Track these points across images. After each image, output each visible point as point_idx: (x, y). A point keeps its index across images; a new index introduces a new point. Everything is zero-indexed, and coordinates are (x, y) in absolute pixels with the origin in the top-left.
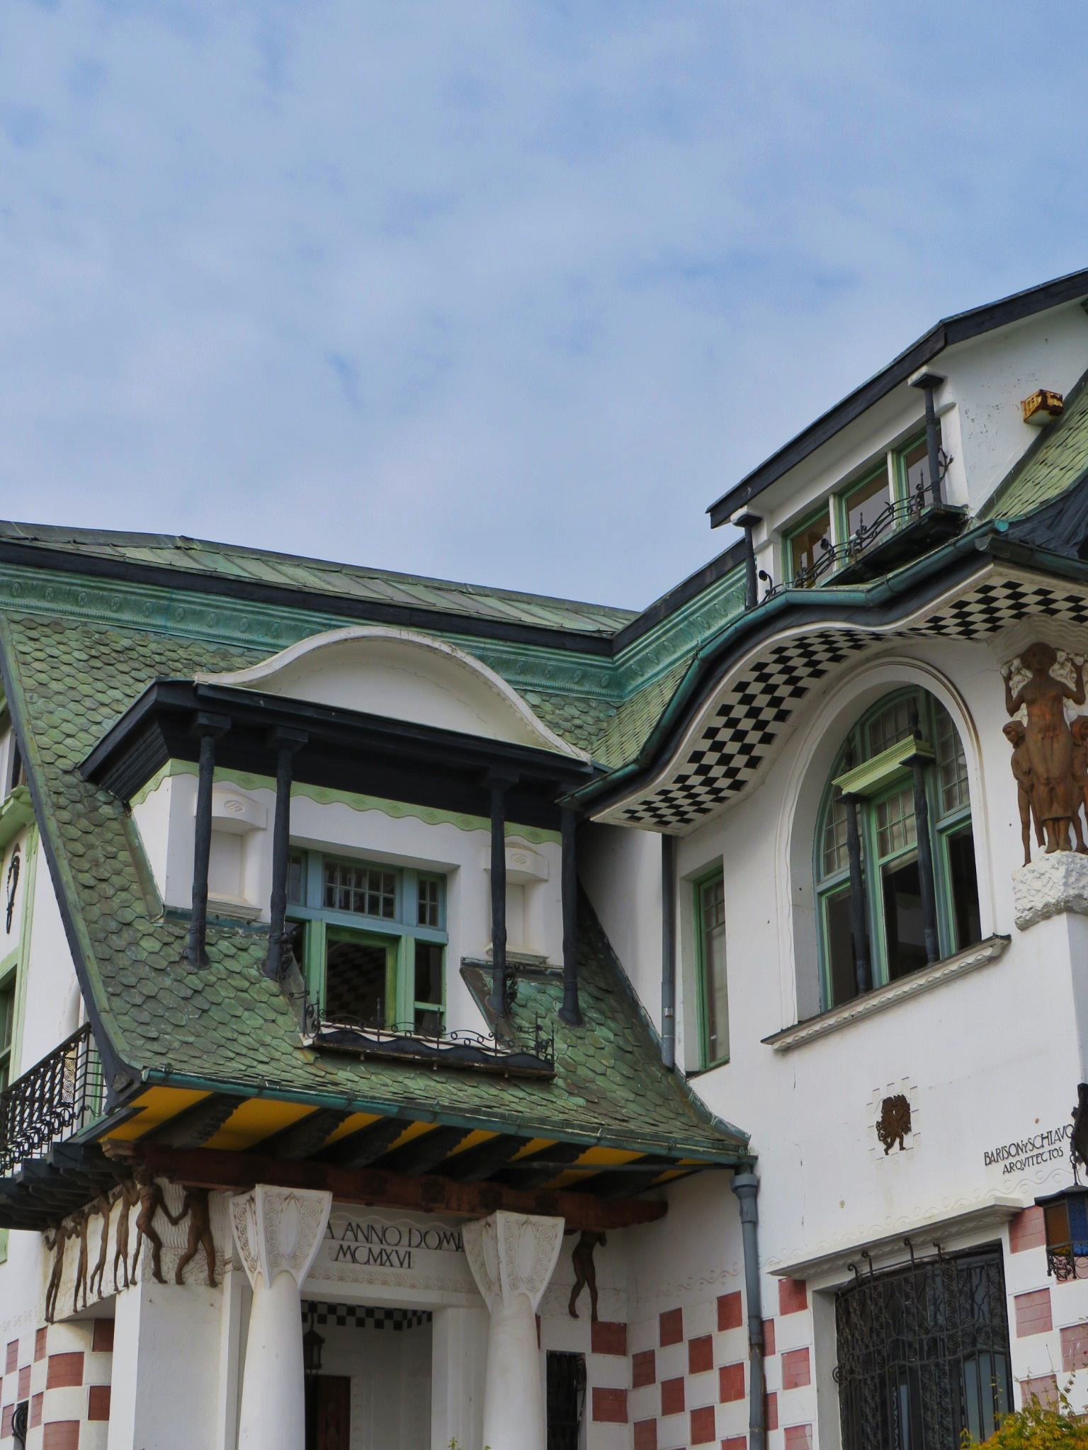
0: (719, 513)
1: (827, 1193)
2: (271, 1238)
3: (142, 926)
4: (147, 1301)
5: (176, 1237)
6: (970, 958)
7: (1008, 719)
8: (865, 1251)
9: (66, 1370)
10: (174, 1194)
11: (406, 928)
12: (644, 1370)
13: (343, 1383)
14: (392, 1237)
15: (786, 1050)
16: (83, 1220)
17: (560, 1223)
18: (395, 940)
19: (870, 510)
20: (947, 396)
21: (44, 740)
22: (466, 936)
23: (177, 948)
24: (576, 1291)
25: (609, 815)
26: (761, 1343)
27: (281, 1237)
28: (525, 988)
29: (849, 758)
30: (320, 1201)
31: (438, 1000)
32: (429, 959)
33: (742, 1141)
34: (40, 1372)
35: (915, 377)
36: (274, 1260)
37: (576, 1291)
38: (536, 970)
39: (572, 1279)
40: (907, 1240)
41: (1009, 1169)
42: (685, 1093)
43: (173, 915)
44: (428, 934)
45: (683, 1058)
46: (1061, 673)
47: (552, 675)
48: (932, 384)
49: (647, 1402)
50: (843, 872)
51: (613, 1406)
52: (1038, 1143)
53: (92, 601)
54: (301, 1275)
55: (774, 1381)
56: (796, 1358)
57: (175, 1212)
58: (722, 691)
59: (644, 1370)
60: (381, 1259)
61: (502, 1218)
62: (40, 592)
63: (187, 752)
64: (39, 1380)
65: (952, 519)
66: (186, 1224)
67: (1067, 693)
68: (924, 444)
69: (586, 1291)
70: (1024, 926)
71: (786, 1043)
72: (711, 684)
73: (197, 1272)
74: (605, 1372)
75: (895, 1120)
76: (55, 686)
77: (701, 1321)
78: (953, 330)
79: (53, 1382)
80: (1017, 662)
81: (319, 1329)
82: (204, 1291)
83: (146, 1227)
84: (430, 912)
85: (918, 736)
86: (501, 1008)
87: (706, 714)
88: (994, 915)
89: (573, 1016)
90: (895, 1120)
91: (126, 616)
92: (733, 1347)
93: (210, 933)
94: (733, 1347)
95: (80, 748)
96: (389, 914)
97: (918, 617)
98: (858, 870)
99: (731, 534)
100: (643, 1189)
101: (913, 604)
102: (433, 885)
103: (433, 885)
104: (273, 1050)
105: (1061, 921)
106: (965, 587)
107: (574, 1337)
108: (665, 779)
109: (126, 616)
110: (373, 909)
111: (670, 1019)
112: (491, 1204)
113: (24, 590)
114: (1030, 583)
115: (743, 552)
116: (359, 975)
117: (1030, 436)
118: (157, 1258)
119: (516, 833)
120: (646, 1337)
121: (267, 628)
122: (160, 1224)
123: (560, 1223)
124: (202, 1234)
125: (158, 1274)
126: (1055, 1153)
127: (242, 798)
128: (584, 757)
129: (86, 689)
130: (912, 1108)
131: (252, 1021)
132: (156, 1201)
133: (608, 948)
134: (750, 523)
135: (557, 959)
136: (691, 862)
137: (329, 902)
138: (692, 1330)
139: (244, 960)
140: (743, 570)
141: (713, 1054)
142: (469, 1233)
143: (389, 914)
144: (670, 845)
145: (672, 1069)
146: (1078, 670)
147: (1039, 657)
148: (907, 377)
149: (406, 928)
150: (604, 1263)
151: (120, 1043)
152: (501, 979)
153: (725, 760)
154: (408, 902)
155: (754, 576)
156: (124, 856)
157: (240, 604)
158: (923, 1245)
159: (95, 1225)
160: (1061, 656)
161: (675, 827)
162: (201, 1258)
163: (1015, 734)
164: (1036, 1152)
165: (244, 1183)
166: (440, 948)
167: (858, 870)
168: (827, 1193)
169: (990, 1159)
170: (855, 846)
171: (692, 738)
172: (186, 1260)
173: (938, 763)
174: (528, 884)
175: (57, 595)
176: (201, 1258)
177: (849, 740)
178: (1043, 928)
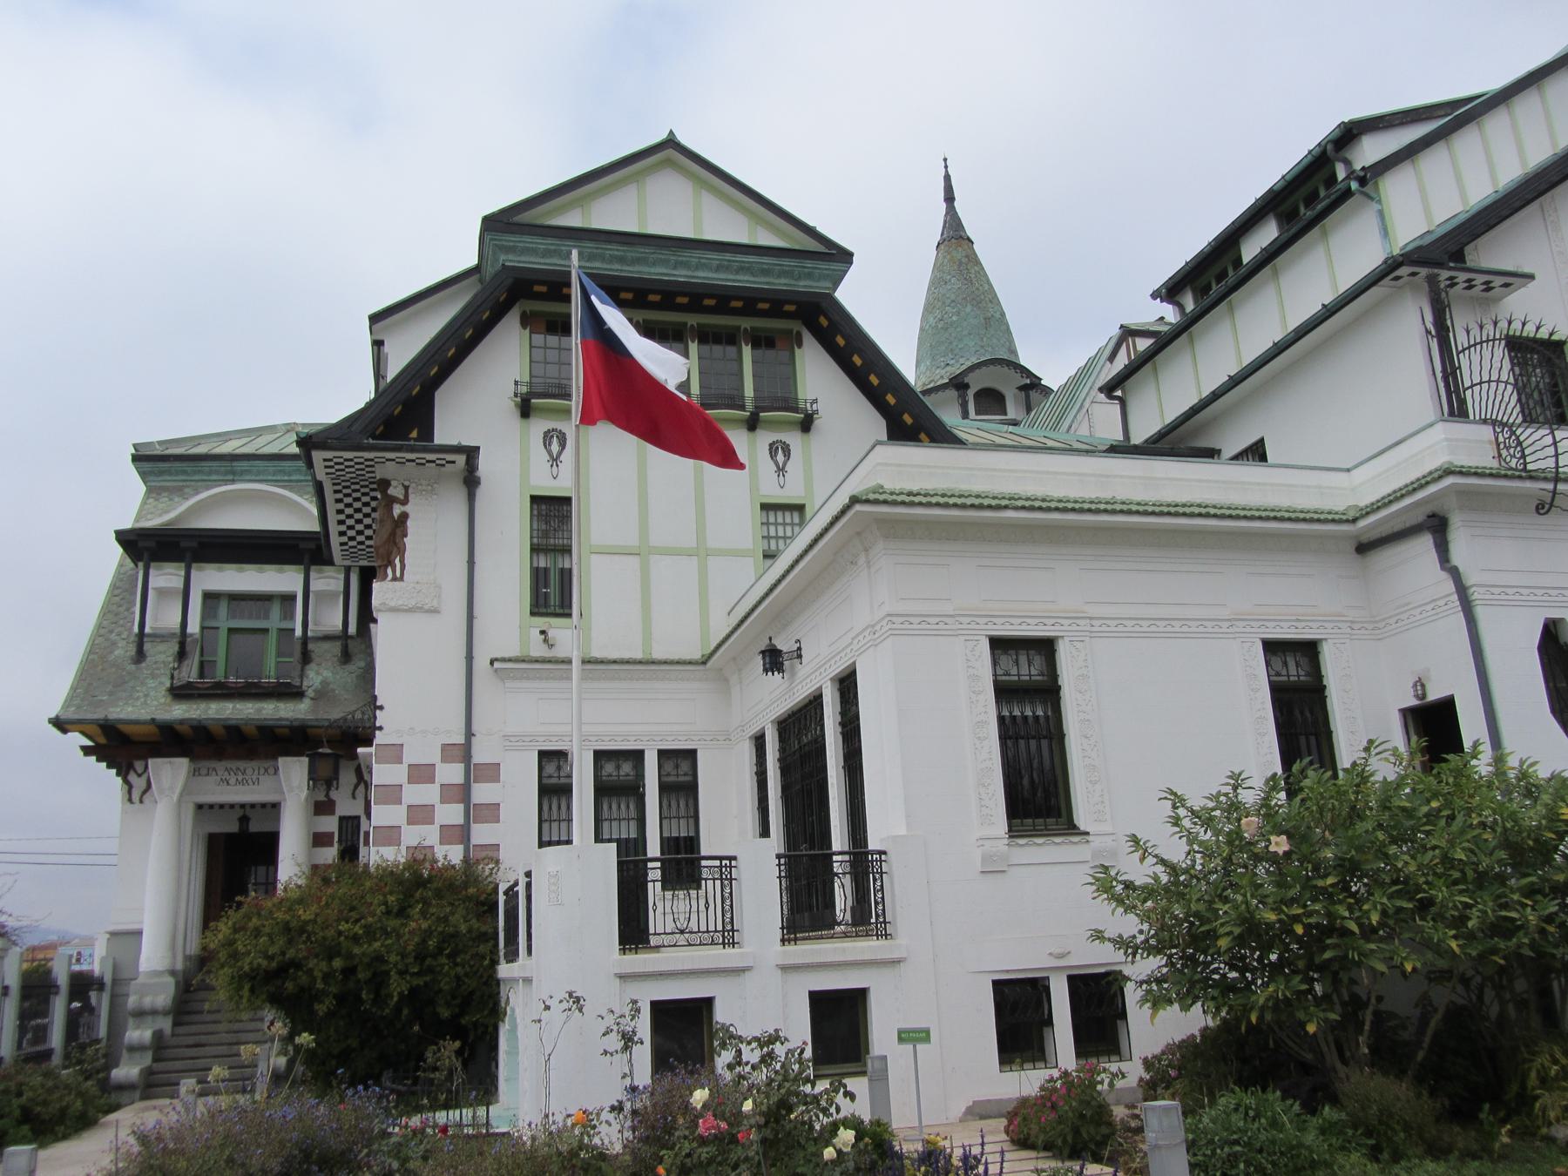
11: (274, 621)
14: (249, 771)
18: (267, 630)
24: (356, 787)
30: (183, 764)
37: (356, 787)
39: (354, 780)
44: (289, 626)
46: (395, 491)
53: (195, 473)
60: (243, 782)
61: (281, 760)
67: (394, 500)
69: (361, 788)
81: (249, 812)
84: (289, 614)
96: (267, 617)
102: (289, 599)
110: (258, 618)
118: (130, 792)
121: (283, 472)
125: (130, 800)
131: (151, 683)
143: (267, 617)
146: (406, 488)
160: (393, 483)
171: (334, 529)
175: (177, 473)
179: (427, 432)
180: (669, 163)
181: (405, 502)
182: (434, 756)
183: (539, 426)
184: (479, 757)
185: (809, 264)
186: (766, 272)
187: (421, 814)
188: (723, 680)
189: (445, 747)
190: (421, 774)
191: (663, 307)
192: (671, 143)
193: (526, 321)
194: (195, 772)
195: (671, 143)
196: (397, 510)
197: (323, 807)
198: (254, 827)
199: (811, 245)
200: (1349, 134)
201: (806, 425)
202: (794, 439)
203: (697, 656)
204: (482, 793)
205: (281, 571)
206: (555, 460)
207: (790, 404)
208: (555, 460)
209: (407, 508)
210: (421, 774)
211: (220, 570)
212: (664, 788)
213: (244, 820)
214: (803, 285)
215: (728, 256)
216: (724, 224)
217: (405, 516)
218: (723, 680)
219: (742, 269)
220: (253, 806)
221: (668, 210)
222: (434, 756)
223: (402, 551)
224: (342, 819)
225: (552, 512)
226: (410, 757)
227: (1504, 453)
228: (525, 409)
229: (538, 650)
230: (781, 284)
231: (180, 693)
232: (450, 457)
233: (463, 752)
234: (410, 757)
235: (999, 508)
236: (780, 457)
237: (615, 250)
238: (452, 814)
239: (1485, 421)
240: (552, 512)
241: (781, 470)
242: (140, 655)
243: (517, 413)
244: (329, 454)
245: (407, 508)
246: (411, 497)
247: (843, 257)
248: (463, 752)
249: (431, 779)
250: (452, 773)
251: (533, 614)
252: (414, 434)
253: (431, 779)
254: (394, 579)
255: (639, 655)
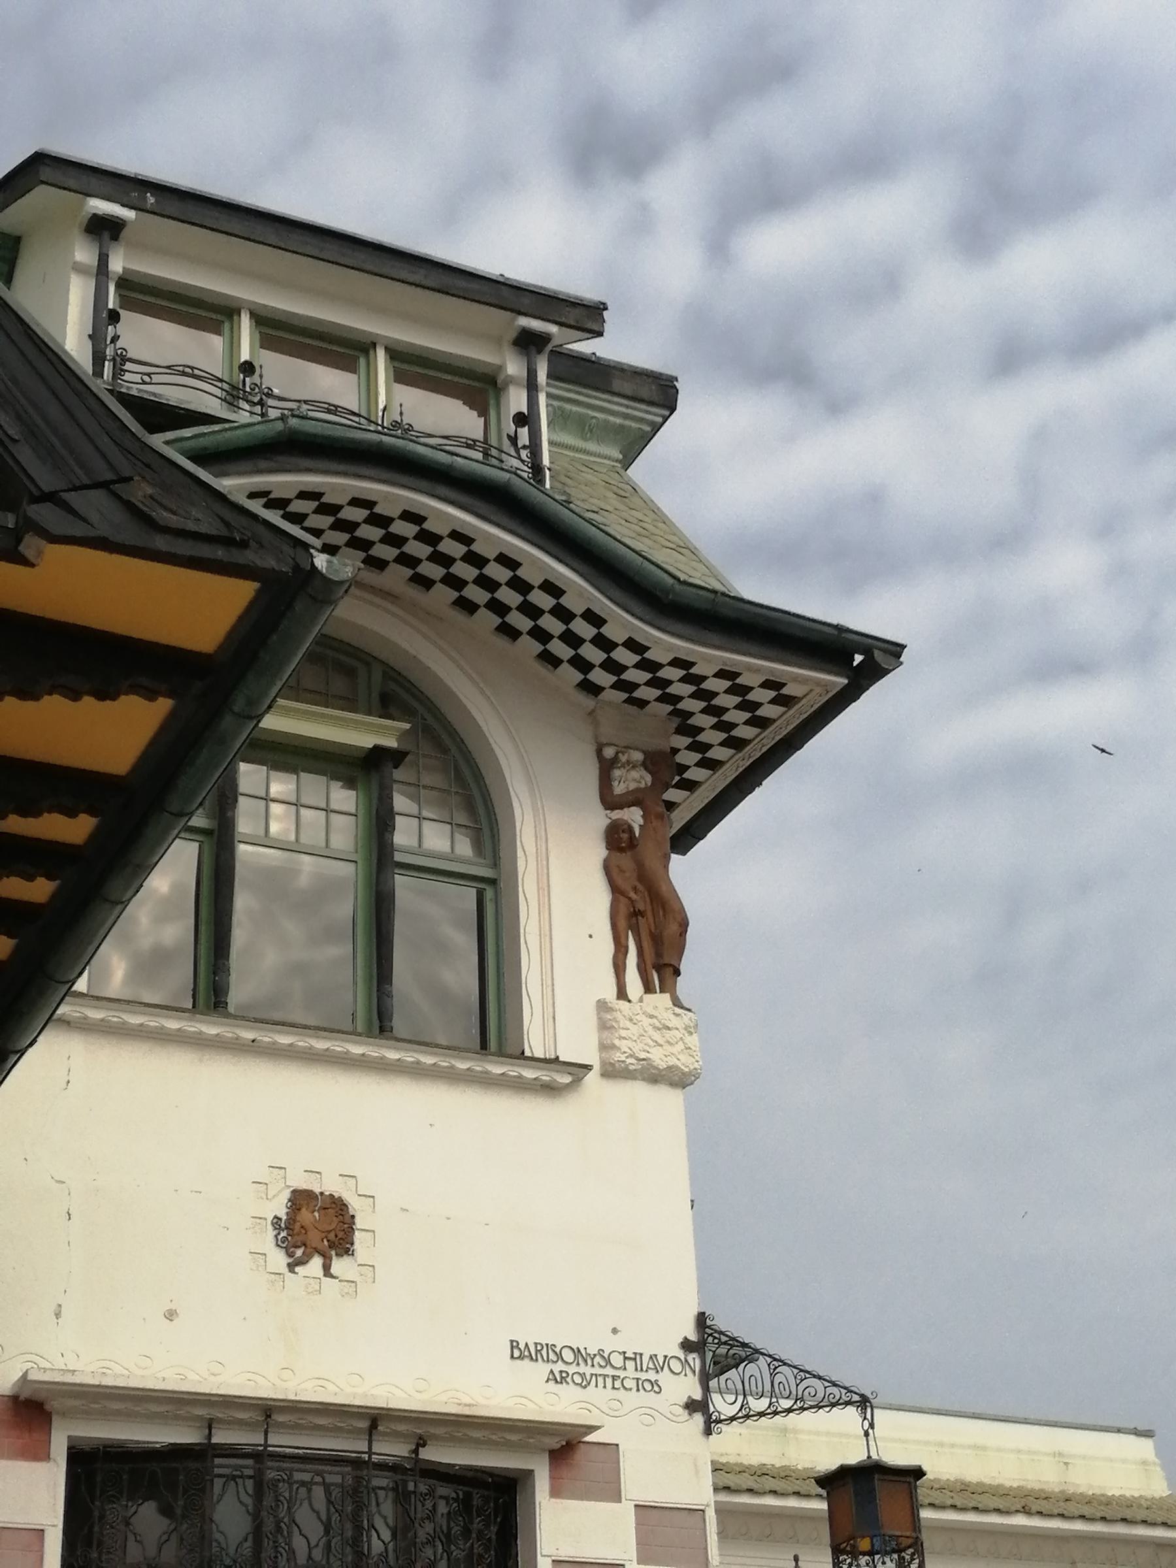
35: (525, 322)
41: (560, 1379)
52: (617, 1360)
72: (263, 464)
80: (638, 756)
101: (715, 638)
126: (648, 1386)
130: (359, 1223)
148: (525, 315)
158: (397, 1435)
164: (609, 1371)
169: (518, 1352)
178: (639, 1090)
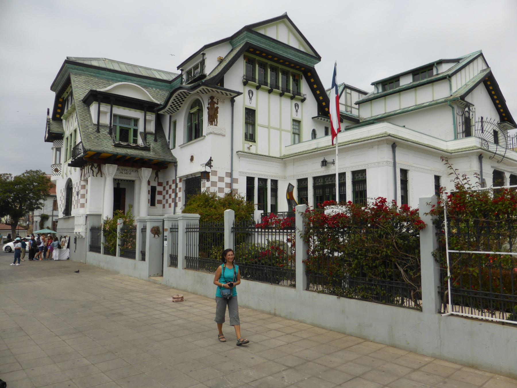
0: (178, 68)
1: (185, 168)
2: (108, 171)
3: (90, 126)
4: (92, 179)
5: (96, 170)
6: (202, 138)
7: (208, 106)
8: (187, 176)
9: (84, 187)
10: (96, 165)
12: (164, 189)
13: (124, 190)
15: (181, 148)
16: (84, 167)
17: (151, 169)
18: (130, 129)
19: (196, 71)
20: (206, 56)
21: (77, 95)
22: (141, 128)
23: (95, 130)
25: (161, 112)
26: (176, 186)
27: (111, 171)
28: (149, 136)
29: (192, 108)
30: (116, 166)
31: (137, 137)
32: (135, 131)
33: (176, 159)
34: (80, 187)
36: (109, 174)
38: (151, 134)
40: (191, 175)
42: (170, 152)
43: (95, 125)
44: (135, 128)
45: (170, 148)
47: (162, 86)
48: (204, 54)
49: (164, 193)
50: (190, 124)
51: (160, 193)
54: (113, 176)
55: (178, 191)
56: (180, 188)
57: (96, 166)
58: (173, 97)
59: (164, 189)
60: (127, 173)
61: (143, 169)
62: (77, 69)
63: (96, 100)
64: (80, 189)
65: (204, 76)
66: (97, 169)
67: (215, 103)
68: (203, 63)
70: (207, 135)
71: (182, 146)
73: (99, 175)
74: (159, 188)
75: (192, 159)
76: (79, 86)
77: (170, 183)
78: (206, 47)
79: (82, 189)
81: (120, 182)
82: (100, 178)
83: (91, 169)
85: (199, 106)
86: (145, 139)
87: (171, 100)
88: (204, 133)
89: (156, 140)
90: (192, 159)
91: (92, 74)
92: (173, 186)
93: (100, 127)
94: (173, 186)
95: (82, 97)
97: (195, 91)
98: (191, 124)
99: (179, 72)
100: (163, 166)
102: (136, 121)
103: (136, 121)
104: (107, 145)
105: (211, 136)
106: (201, 88)
107: (154, 184)
108: (167, 108)
109: (92, 74)
111: (169, 142)
112: (141, 167)
113: (75, 69)
114: (209, 88)
115: (181, 75)
116: (124, 134)
117: (217, 63)
119: (148, 114)
120: (164, 184)
121: (115, 77)
122: (94, 169)
123: (151, 169)
124: (100, 170)
127: (105, 108)
128: (159, 103)
129: (84, 87)
132: (93, 166)
133: (163, 130)
134: (182, 70)
135: (154, 132)
136: (173, 120)
137: (120, 123)
138: (169, 184)
139: (104, 132)
140: (180, 78)
141: (174, 147)
142: (139, 170)
144: (170, 116)
145: (169, 148)
147: (212, 98)
149: (132, 127)
150: (160, 175)
151: (84, 145)
152: (145, 135)
153: (175, 106)
154: (133, 123)
155: (182, 78)
156: (88, 115)
157: (111, 73)
159: (86, 168)
161: (171, 114)
162: (100, 173)
163: (208, 108)
165: (105, 164)
166: (137, 130)
167: (191, 124)
168: (185, 168)
170: (191, 121)
171: (170, 103)
172: (97, 173)
173: (200, 111)
174: (150, 121)
176: (100, 173)
177: (192, 105)
179: (222, 85)
180: (284, 22)
181: (217, 104)
182: (224, 175)
183: (247, 89)
184: (234, 176)
185: (312, 59)
186: (302, 59)
187: (221, 190)
188: (285, 165)
189: (226, 173)
190: (221, 179)
191: (274, 60)
192: (285, 16)
193: (245, 57)
194: (118, 169)
195: (285, 16)
196: (216, 106)
197: (149, 183)
198: (121, 186)
199: (312, 53)
200: (440, 62)
201: (303, 100)
202: (299, 103)
203: (278, 156)
204: (235, 186)
205: (136, 111)
206: (251, 99)
207: (299, 94)
208: (251, 99)
209: (218, 106)
210: (221, 179)
211: (118, 108)
212: (272, 189)
213: (118, 184)
214: (309, 64)
215: (296, 53)
216: (294, 43)
217: (217, 108)
218: (285, 165)
219: (298, 57)
220: (121, 180)
221: (281, 34)
222: (224, 175)
223: (217, 118)
224: (152, 187)
225: (250, 114)
226: (219, 174)
227: (483, 145)
228: (245, 84)
229: (246, 150)
230: (305, 63)
231: (117, 146)
232: (232, 94)
233: (230, 175)
234: (219, 174)
235: (408, 141)
236: (297, 108)
237: (273, 44)
238: (227, 190)
239: (479, 138)
240: (250, 114)
241: (297, 111)
242: (98, 131)
243: (242, 84)
244: (205, 87)
245: (218, 106)
246: (219, 103)
247: (318, 58)
248: (230, 175)
249: (223, 181)
250: (228, 180)
251: (245, 140)
252: (219, 85)
253: (223, 181)
254: (215, 125)
255: (267, 155)
